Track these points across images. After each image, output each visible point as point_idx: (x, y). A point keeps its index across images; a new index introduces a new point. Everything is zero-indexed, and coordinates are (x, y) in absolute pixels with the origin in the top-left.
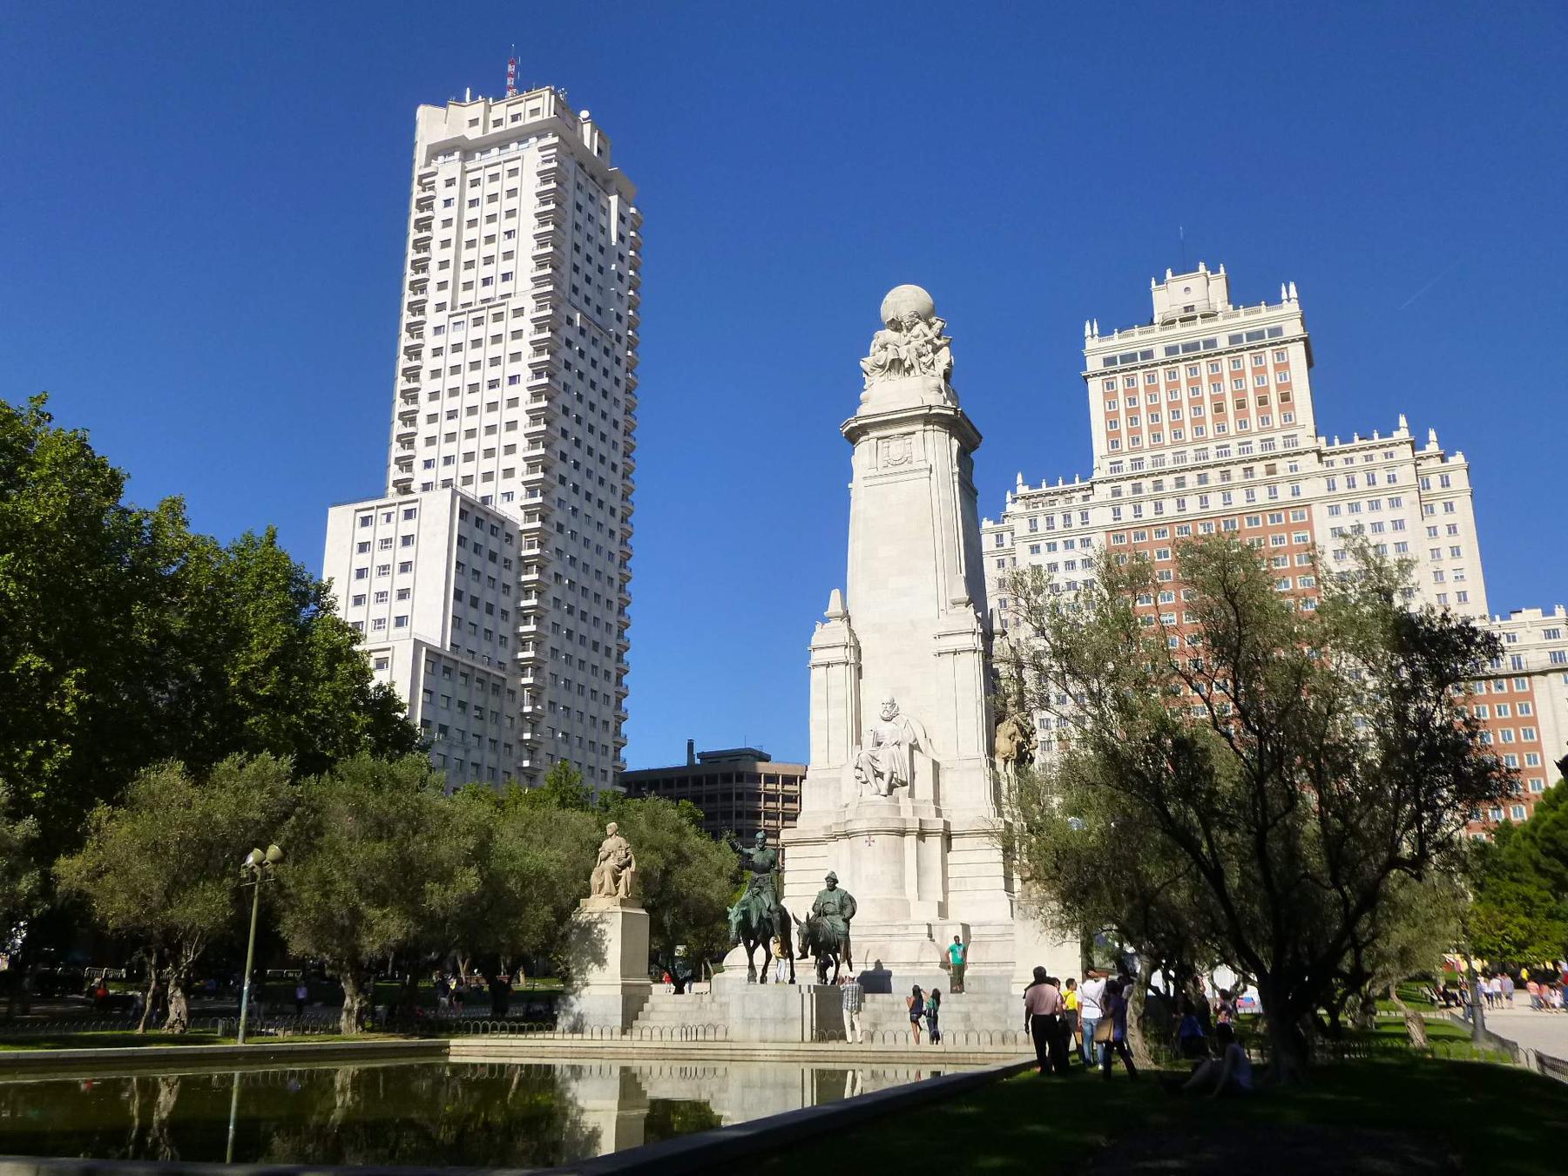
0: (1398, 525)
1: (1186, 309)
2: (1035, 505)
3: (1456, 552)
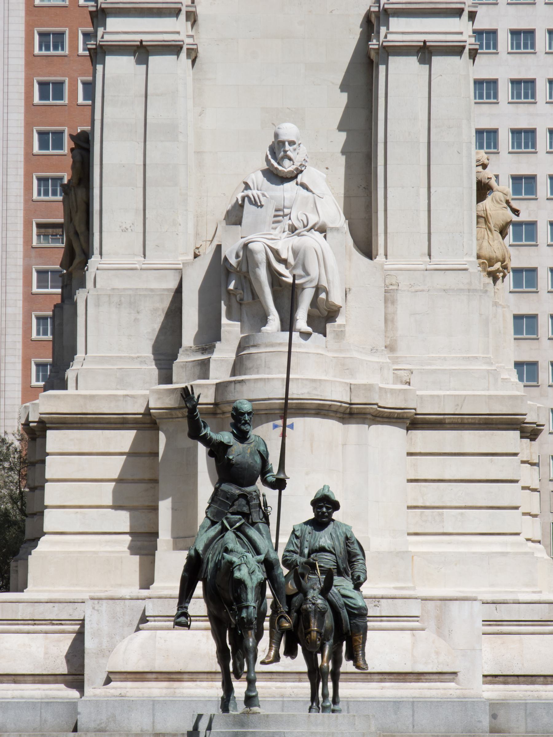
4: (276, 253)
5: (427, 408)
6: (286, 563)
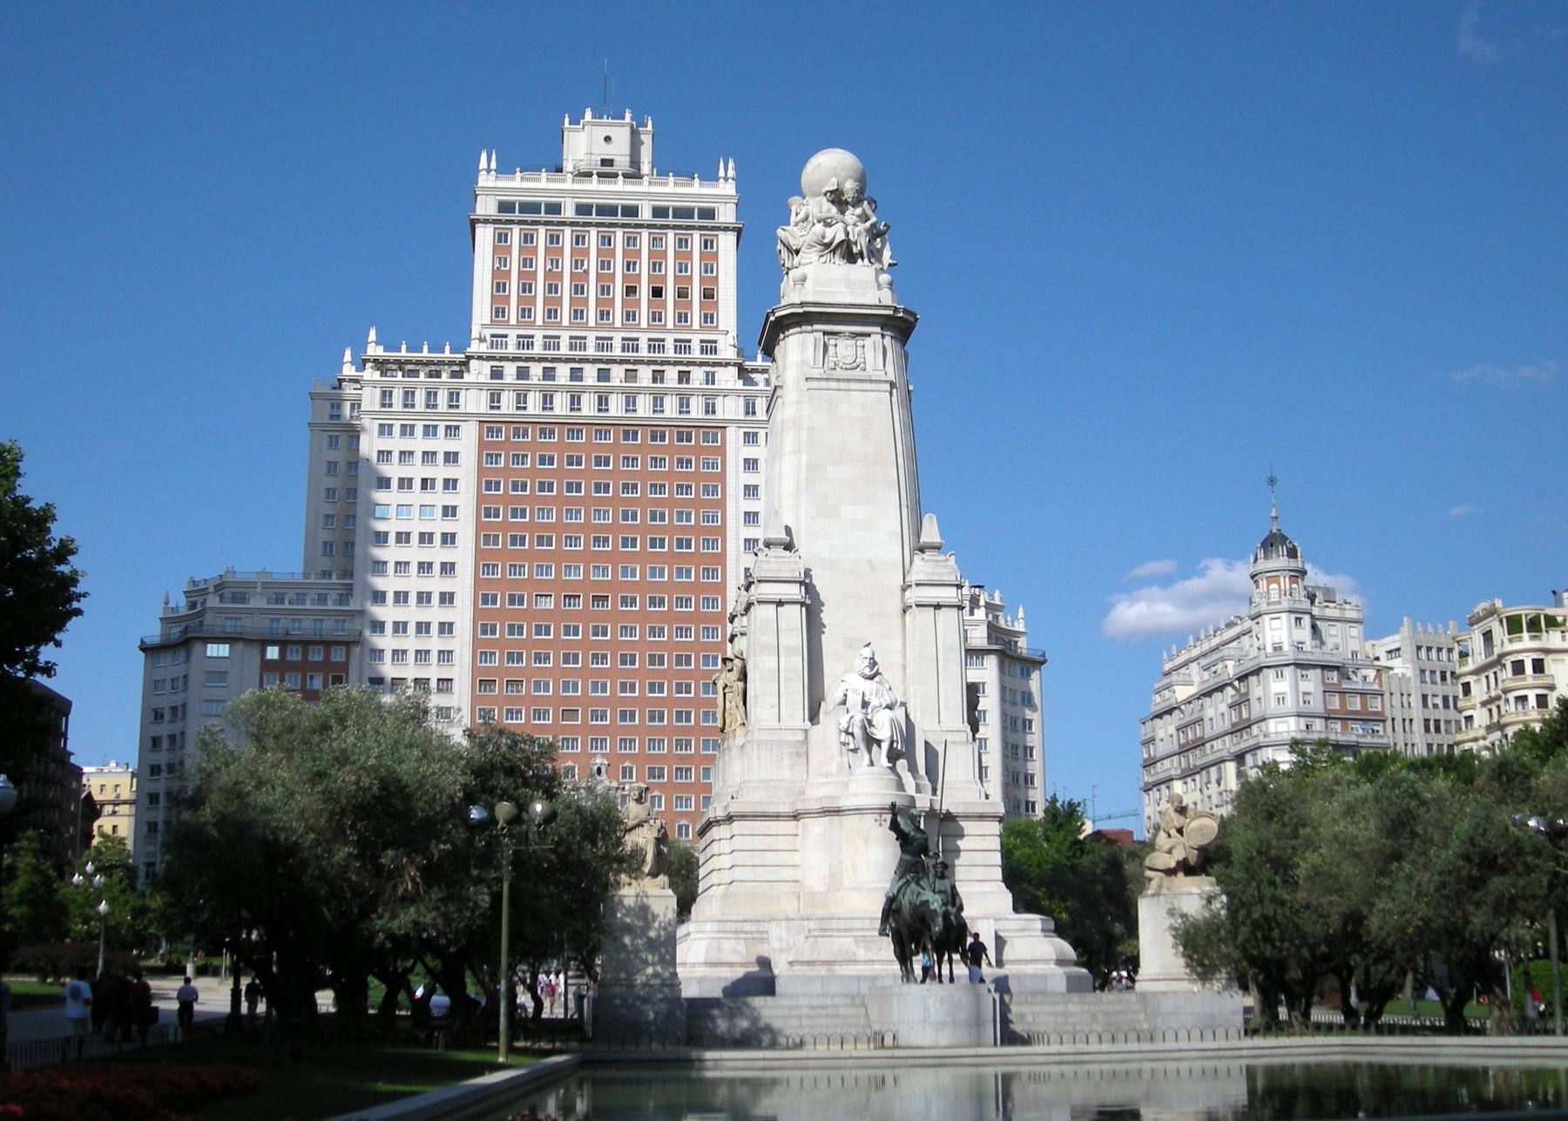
1: (607, 162)
4: (870, 722)
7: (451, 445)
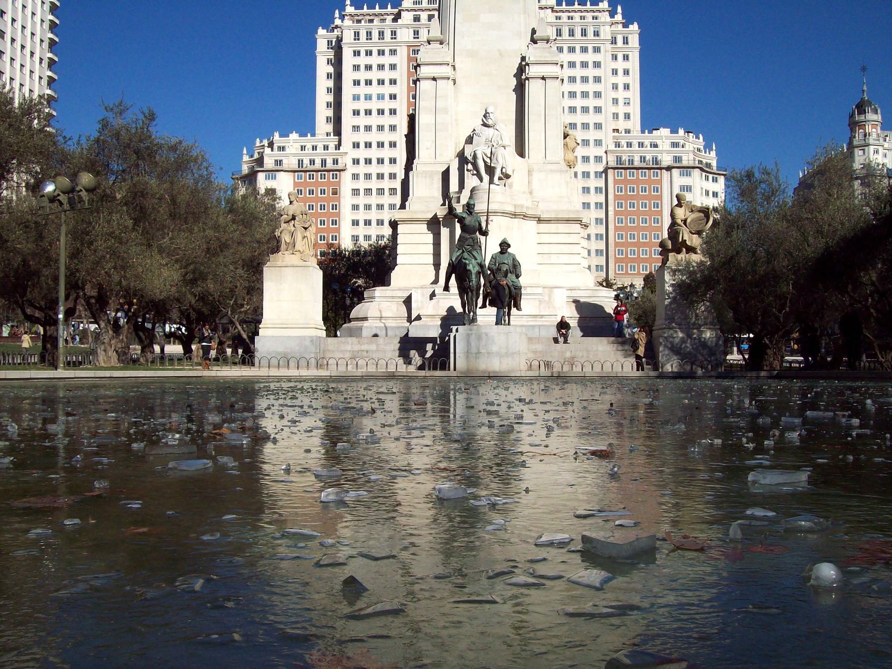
0: (597, 65)
2: (359, 21)
3: (627, 87)
5: (544, 216)
6: (489, 269)
7: (393, 60)
